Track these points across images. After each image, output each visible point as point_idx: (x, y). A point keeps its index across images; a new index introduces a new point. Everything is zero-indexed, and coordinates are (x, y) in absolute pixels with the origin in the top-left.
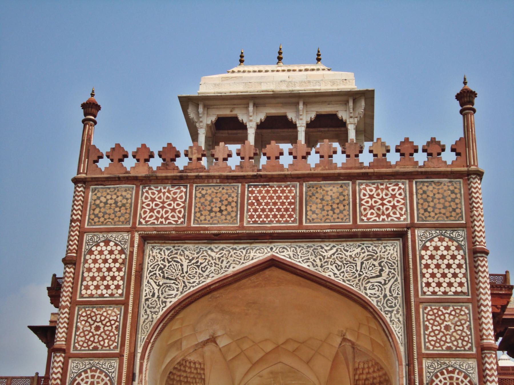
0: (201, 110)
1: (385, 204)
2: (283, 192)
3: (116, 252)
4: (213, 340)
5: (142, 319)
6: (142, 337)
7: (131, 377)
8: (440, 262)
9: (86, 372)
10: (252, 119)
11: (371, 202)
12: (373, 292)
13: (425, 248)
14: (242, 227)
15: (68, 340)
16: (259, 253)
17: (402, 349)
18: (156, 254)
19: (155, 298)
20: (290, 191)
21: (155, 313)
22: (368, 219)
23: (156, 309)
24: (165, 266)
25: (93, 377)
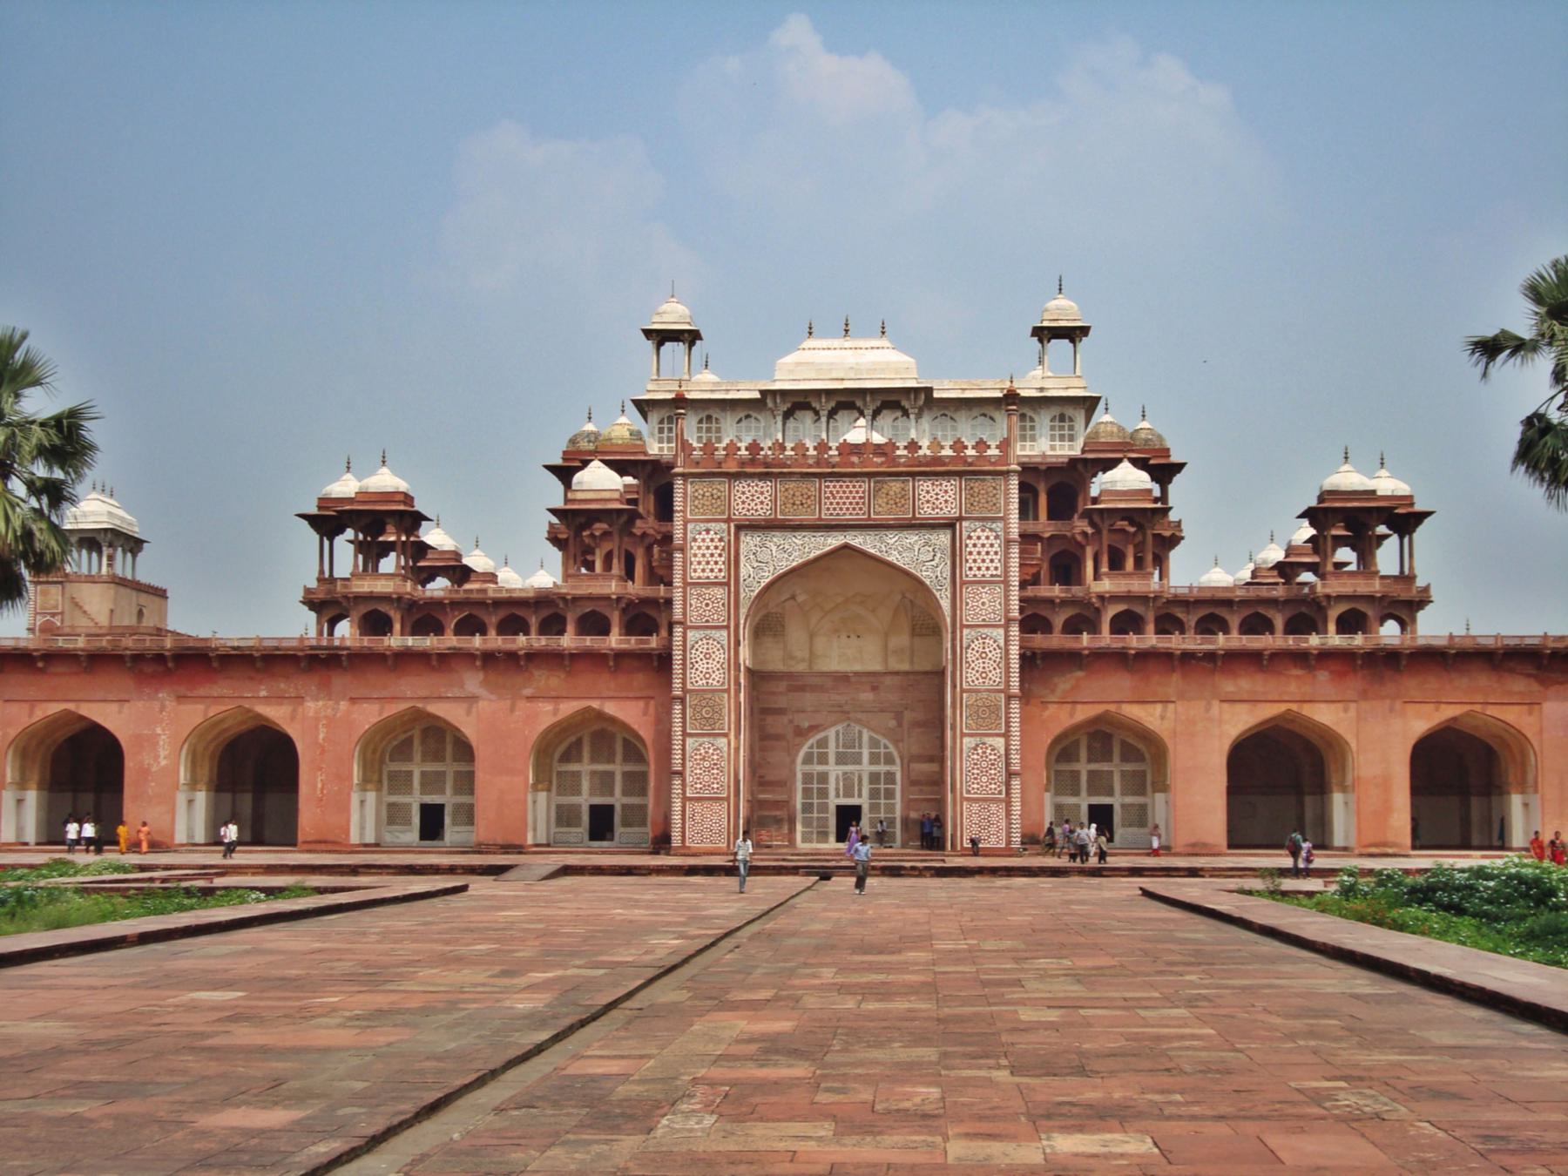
4: (793, 597)
6: (743, 611)
7: (738, 643)
13: (970, 537)
14: (820, 519)
15: (684, 614)
16: (834, 541)
17: (948, 620)
18: (749, 542)
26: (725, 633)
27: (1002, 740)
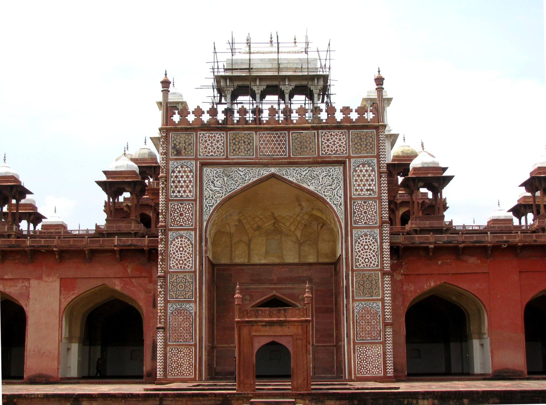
0: (228, 84)
1: (335, 143)
2: (279, 137)
3: (188, 172)
5: (204, 210)
6: (206, 218)
8: (363, 178)
9: (177, 238)
10: (258, 89)
11: (328, 143)
12: (328, 194)
16: (265, 172)
19: (210, 198)
20: (283, 137)
21: (211, 206)
22: (326, 153)
23: (212, 204)
24: (214, 180)
25: (181, 241)
26: (193, 233)
27: (380, 304)
